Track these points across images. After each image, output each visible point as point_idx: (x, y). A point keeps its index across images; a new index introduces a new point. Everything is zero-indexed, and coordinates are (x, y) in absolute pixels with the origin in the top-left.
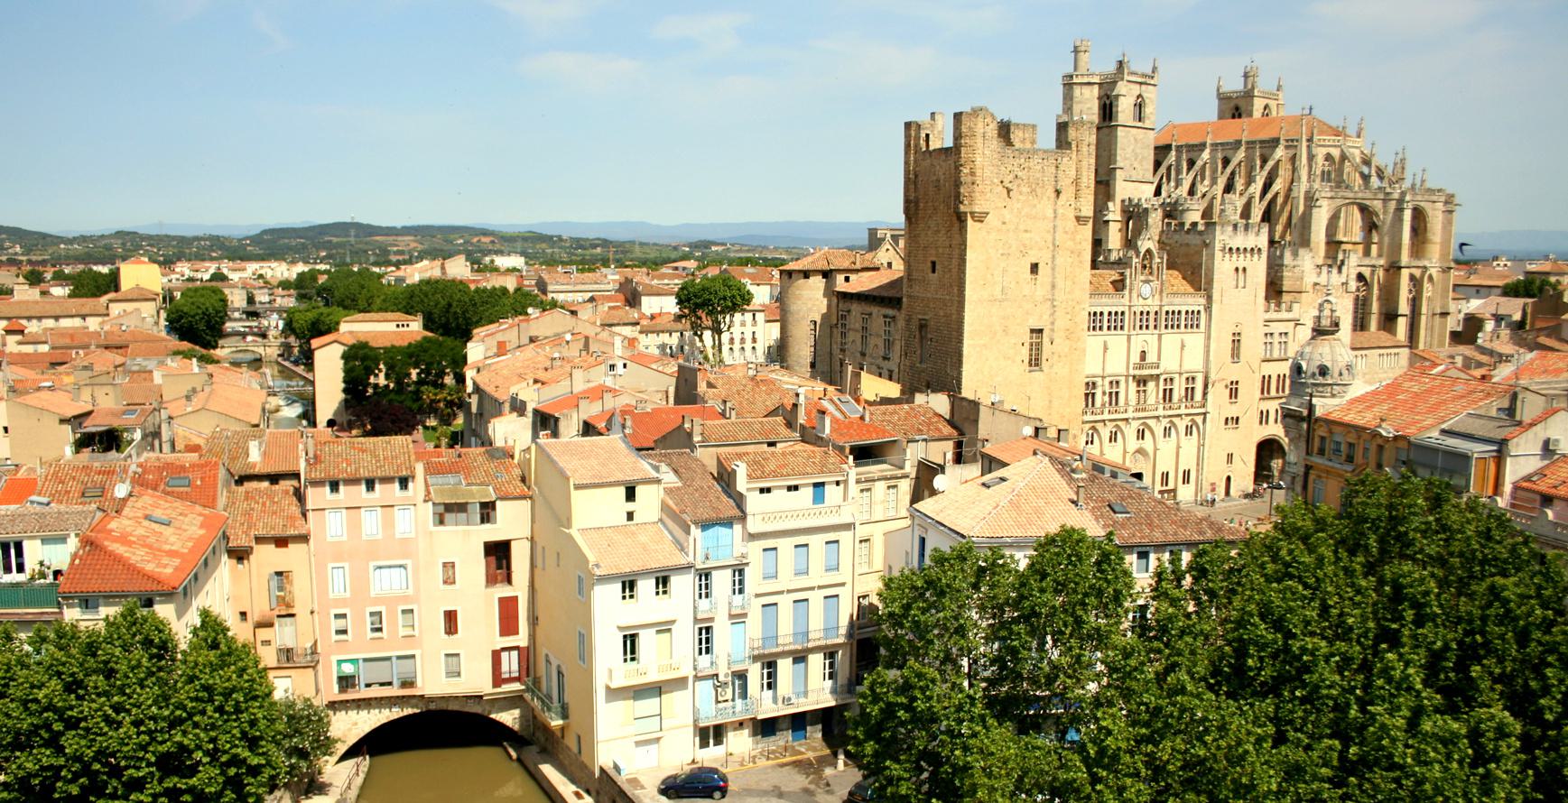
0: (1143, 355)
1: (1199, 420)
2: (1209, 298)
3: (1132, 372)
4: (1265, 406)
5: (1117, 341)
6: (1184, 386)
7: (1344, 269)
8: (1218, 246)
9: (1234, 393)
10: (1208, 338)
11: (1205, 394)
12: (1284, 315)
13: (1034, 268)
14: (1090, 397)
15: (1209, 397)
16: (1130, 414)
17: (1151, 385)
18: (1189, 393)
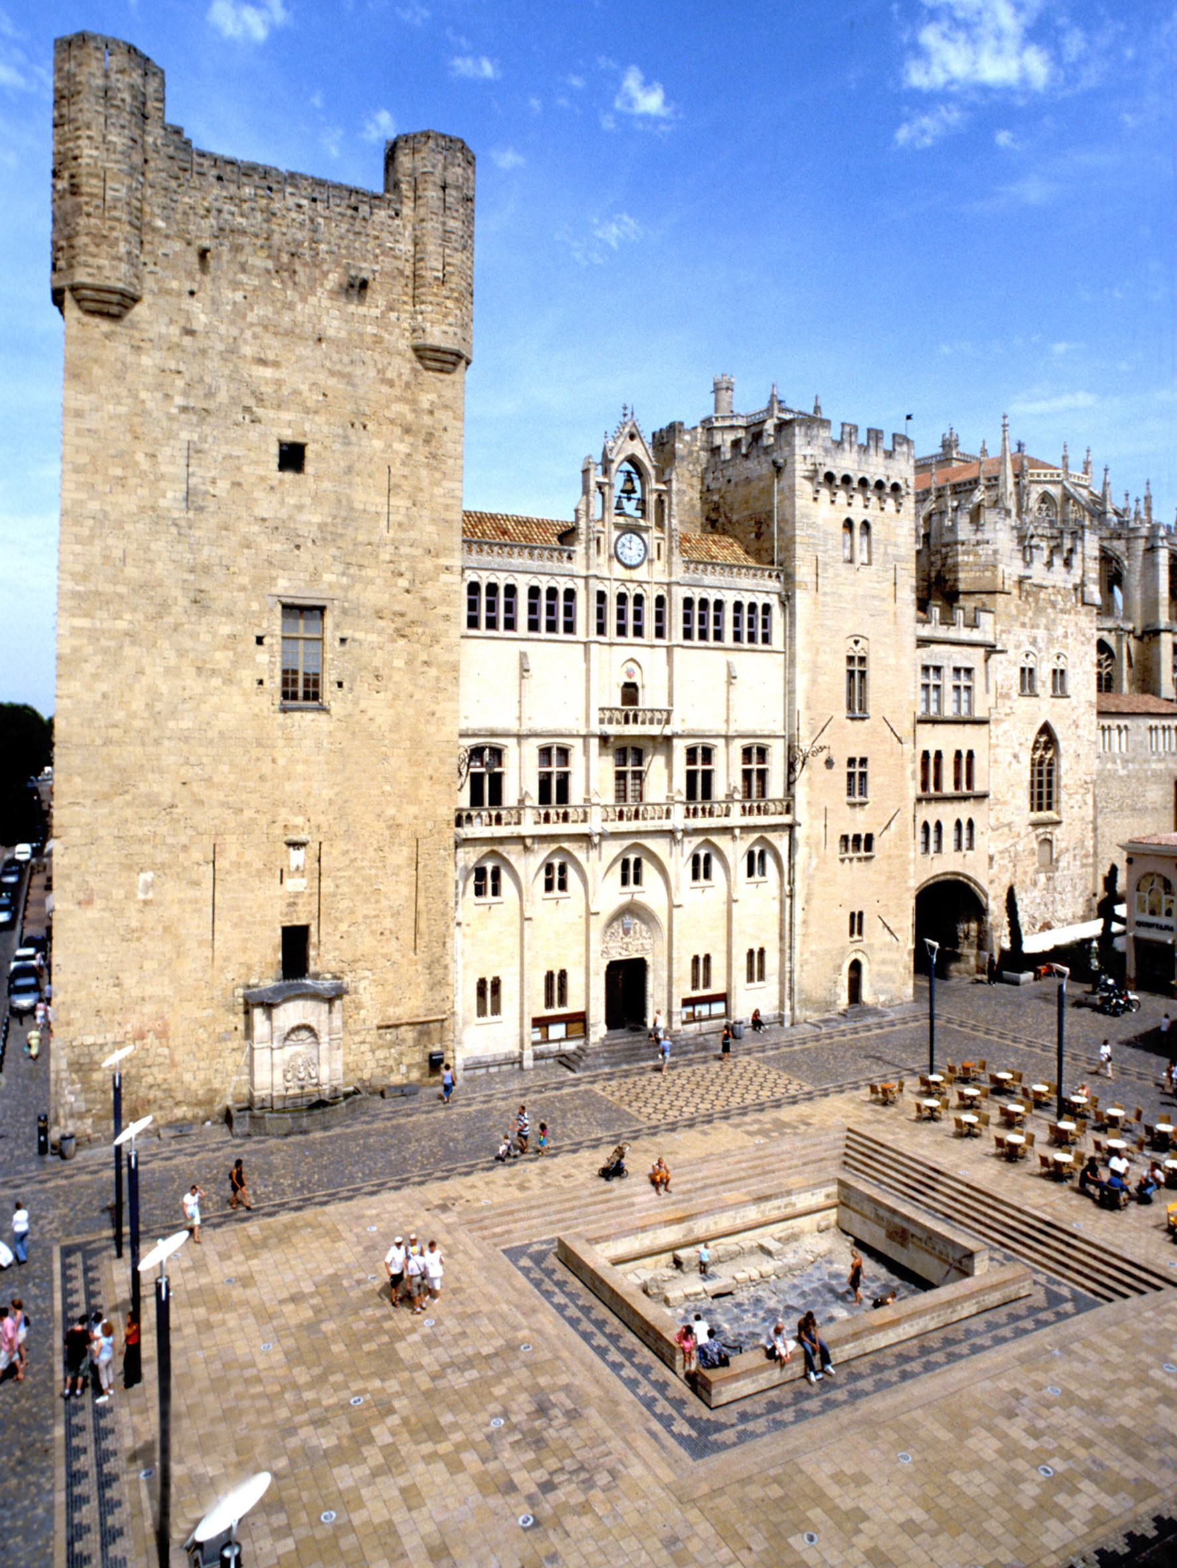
0: (630, 692)
1: (781, 842)
2: (789, 579)
3: (596, 728)
4: (931, 813)
5: (553, 656)
6: (738, 766)
7: (1076, 560)
8: (801, 468)
9: (857, 780)
10: (791, 663)
11: (790, 784)
12: (965, 634)
13: (292, 457)
14: (486, 789)
15: (800, 790)
16: (595, 825)
17: (655, 765)
18: (754, 780)
